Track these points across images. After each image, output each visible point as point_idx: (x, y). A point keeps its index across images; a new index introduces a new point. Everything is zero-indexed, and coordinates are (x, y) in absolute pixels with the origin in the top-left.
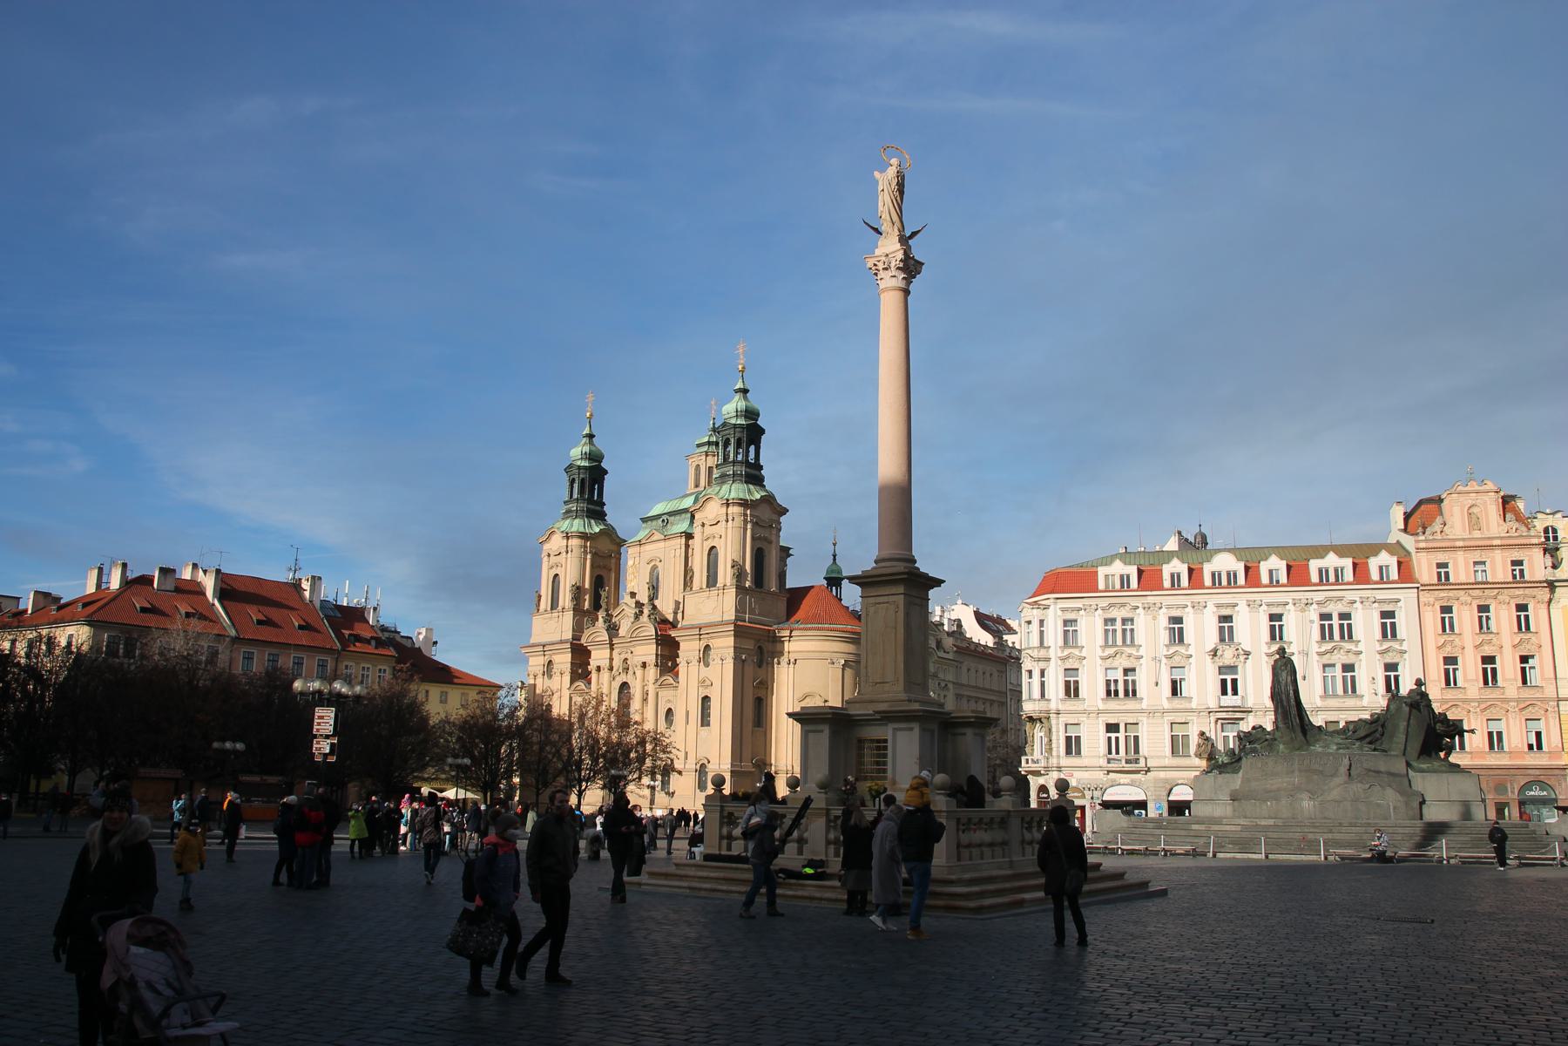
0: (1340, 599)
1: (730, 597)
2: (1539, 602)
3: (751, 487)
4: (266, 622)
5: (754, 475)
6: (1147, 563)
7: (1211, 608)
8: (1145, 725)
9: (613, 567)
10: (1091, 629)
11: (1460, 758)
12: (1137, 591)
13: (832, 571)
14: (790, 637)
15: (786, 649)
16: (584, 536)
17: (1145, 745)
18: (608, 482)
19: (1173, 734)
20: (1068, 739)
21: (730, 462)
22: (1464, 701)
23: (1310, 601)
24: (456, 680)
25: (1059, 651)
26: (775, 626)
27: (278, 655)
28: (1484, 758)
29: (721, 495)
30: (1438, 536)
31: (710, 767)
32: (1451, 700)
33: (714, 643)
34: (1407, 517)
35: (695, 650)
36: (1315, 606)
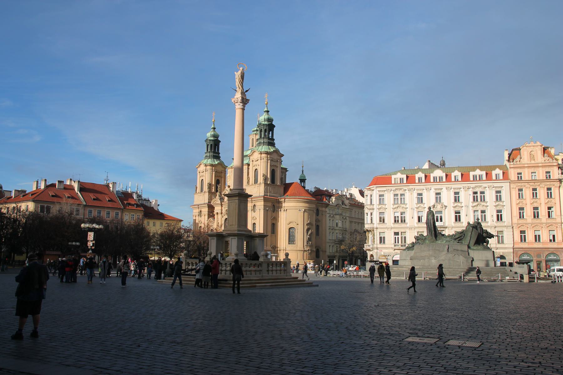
0: (481, 186)
1: (262, 187)
2: (555, 187)
3: (270, 147)
5: (271, 143)
6: (411, 174)
7: (433, 190)
8: (408, 233)
9: (223, 176)
10: (389, 198)
11: (524, 245)
13: (302, 177)
14: (285, 201)
15: (283, 206)
16: (212, 165)
17: (408, 240)
18: (221, 145)
20: (381, 238)
21: (262, 138)
22: (526, 224)
23: (469, 187)
24: (165, 219)
25: (377, 206)
27: (101, 211)
28: (533, 244)
29: (259, 150)
30: (518, 163)
32: (521, 223)
33: (257, 204)
34: (510, 155)
35: (197, 212)
36: (471, 189)
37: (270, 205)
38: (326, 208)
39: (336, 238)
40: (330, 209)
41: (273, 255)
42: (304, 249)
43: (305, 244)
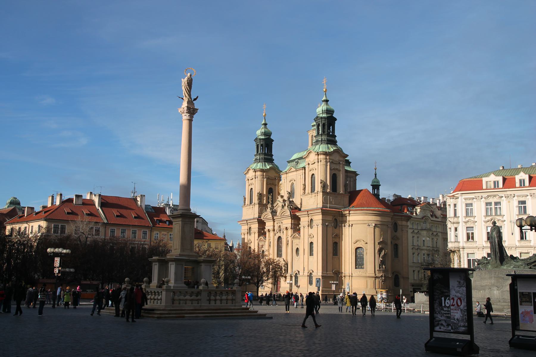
3: (329, 146)
4: (121, 216)
5: (332, 140)
6: (509, 175)
10: (479, 208)
12: (502, 189)
13: (374, 182)
14: (349, 214)
15: (348, 220)
16: (262, 171)
18: (274, 144)
21: (320, 135)
24: (205, 238)
26: (342, 209)
29: (315, 150)
31: (313, 274)
37: (331, 219)
38: (407, 222)
39: (423, 261)
41: (332, 282)
42: (375, 275)
43: (377, 268)
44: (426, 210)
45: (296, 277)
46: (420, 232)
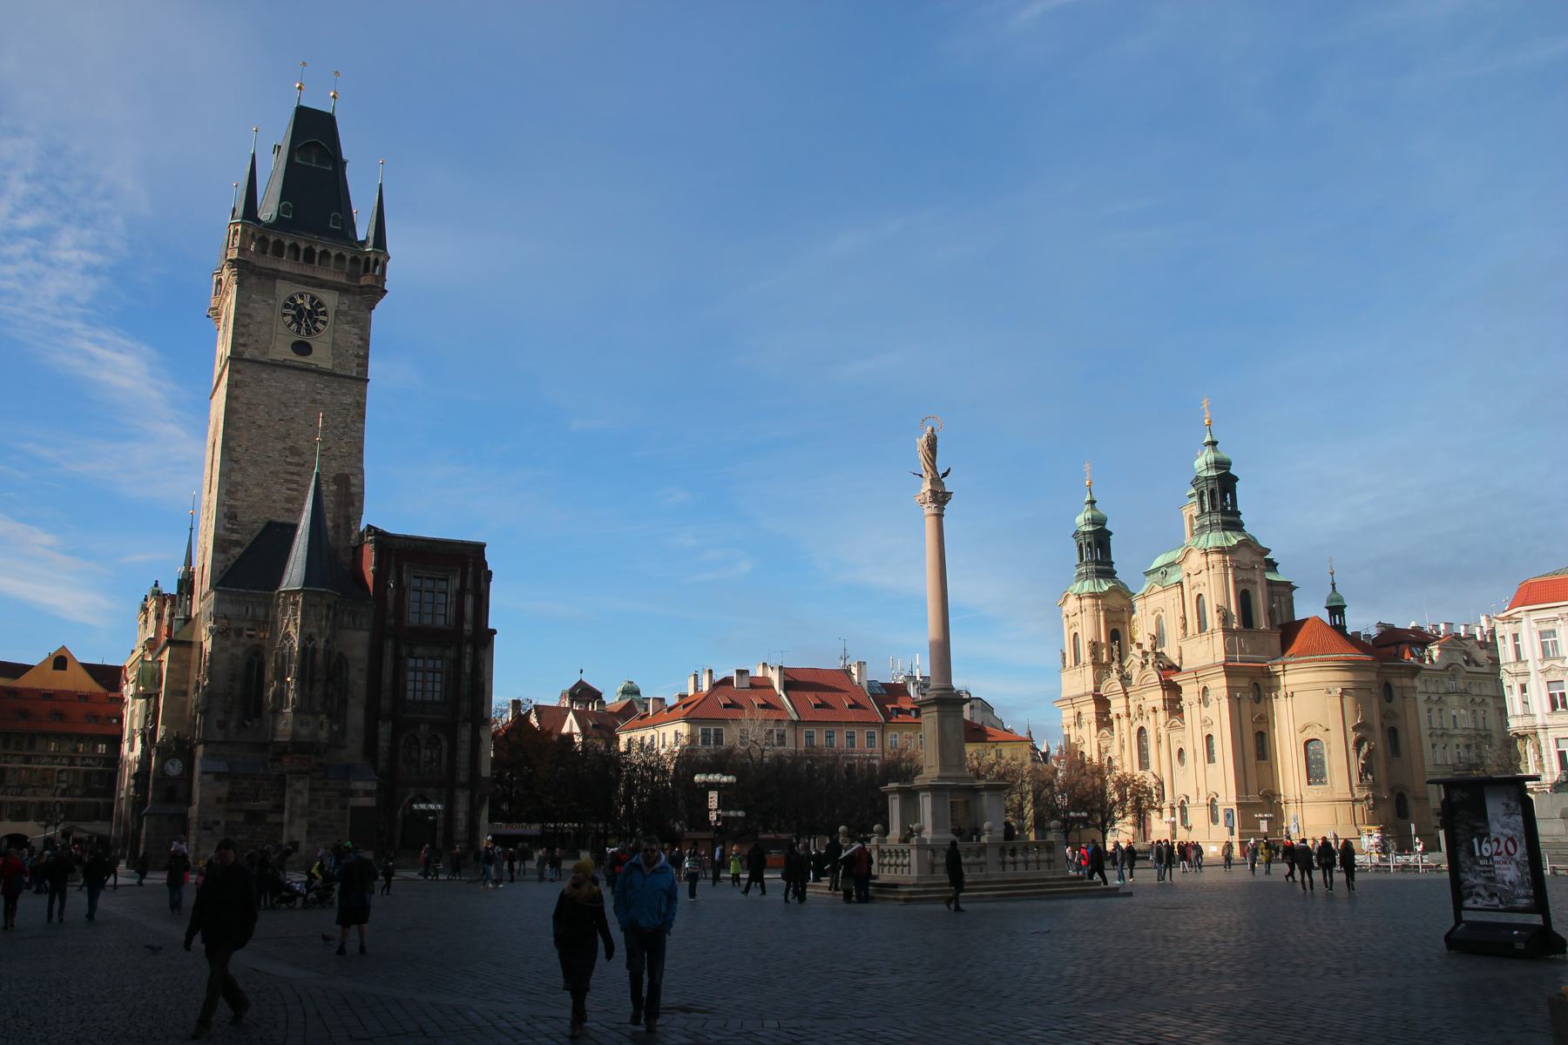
1: (1218, 643)
3: (1228, 533)
4: (822, 705)
5: (1232, 522)
13: (1332, 600)
14: (1285, 671)
15: (1282, 683)
16: (1094, 596)
19: (1559, 750)
24: (989, 739)
26: (1269, 663)
27: (833, 732)
31: (1218, 800)
39: (1456, 761)
40: (1426, 681)
41: (1260, 815)
42: (1353, 795)
43: (1355, 781)
44: (1454, 650)
45: (1183, 809)
46: (1444, 698)
